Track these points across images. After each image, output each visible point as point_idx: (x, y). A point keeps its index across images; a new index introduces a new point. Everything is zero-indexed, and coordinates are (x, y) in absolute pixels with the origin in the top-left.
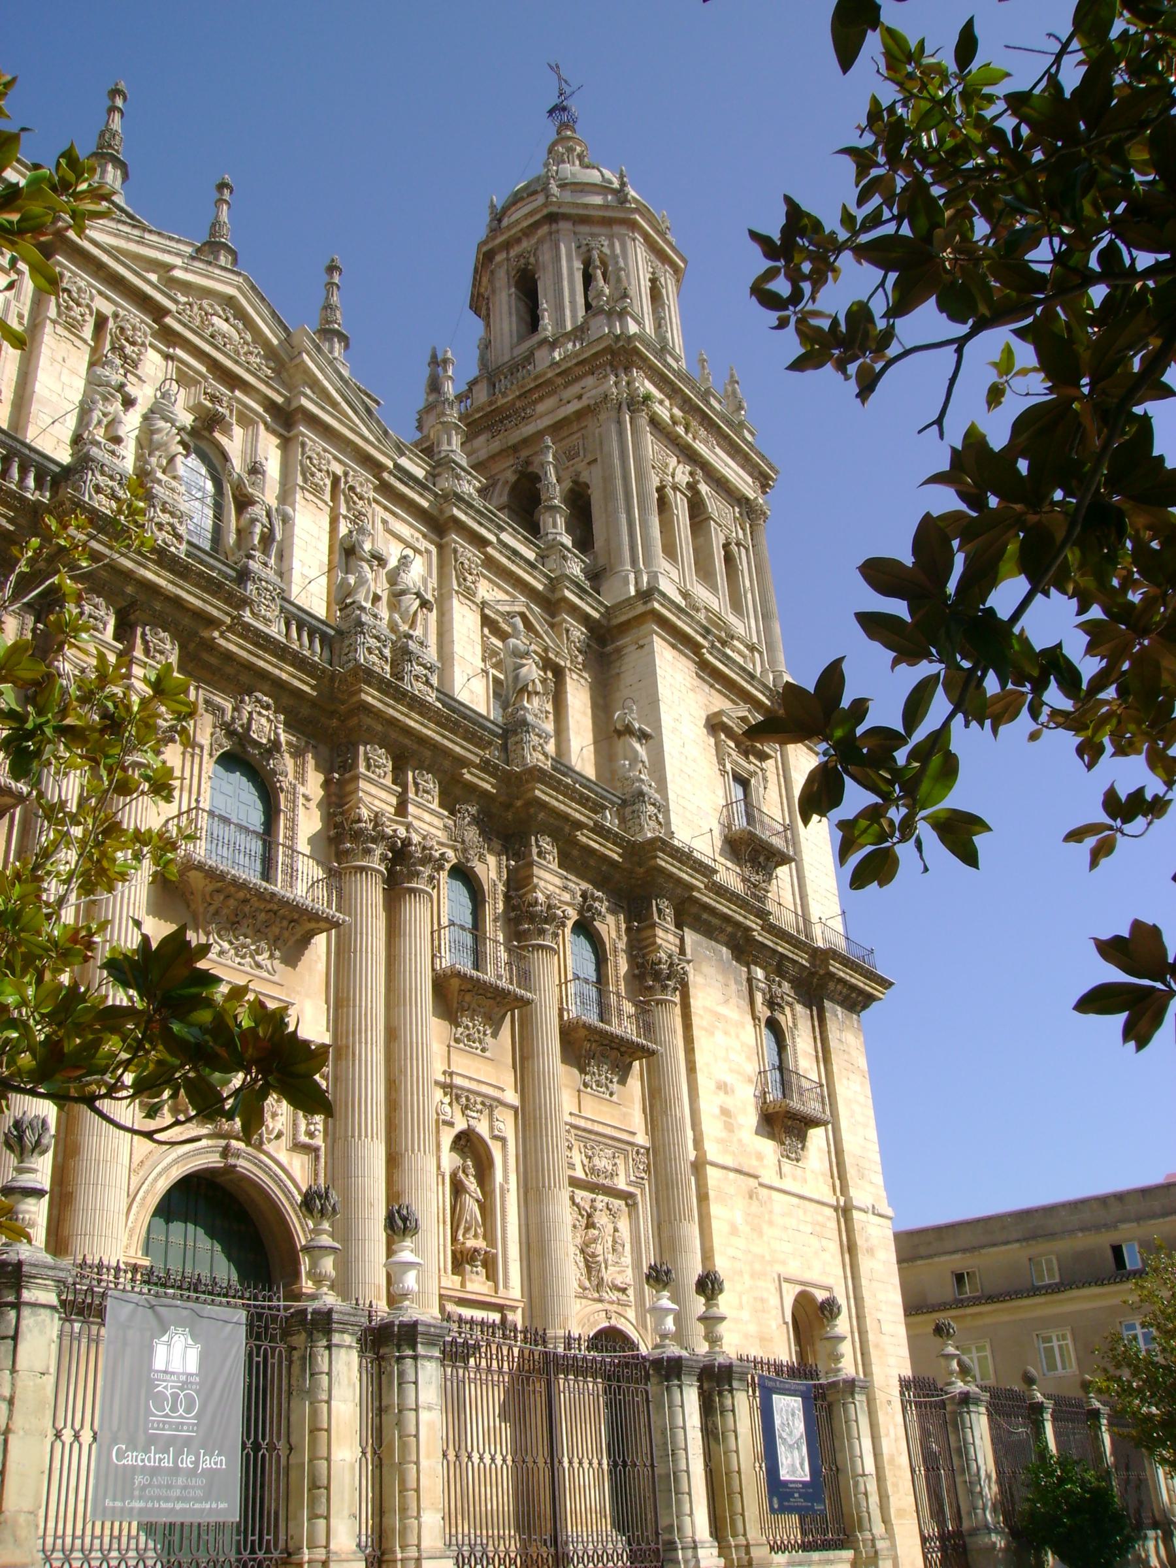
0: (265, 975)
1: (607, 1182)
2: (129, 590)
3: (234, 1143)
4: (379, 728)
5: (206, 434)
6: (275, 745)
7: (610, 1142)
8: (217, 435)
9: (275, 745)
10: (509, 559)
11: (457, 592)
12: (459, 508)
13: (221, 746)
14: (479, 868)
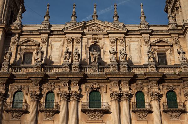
14: (143, 91)
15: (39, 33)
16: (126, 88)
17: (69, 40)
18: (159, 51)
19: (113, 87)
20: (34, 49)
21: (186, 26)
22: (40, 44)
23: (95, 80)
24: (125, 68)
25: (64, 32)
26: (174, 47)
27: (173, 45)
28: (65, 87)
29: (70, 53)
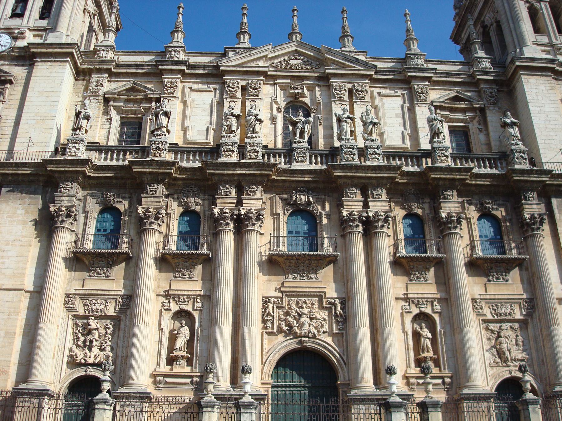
0: (314, 280)
1: (509, 317)
2: (236, 178)
3: (303, 339)
4: (349, 181)
5: (297, 101)
6: (309, 203)
7: (508, 301)
8: (301, 99)
9: (309, 203)
10: (446, 77)
11: (417, 104)
12: (410, 72)
13: (289, 210)
15: (159, 72)
16: (379, 204)
17: (233, 88)
18: (453, 122)
19: (349, 201)
20: (147, 110)
21: (518, 63)
22: (160, 97)
23: (303, 185)
24: (377, 156)
25: (222, 68)
26: (487, 112)
27: (486, 108)
28: (226, 198)
29: (238, 117)
